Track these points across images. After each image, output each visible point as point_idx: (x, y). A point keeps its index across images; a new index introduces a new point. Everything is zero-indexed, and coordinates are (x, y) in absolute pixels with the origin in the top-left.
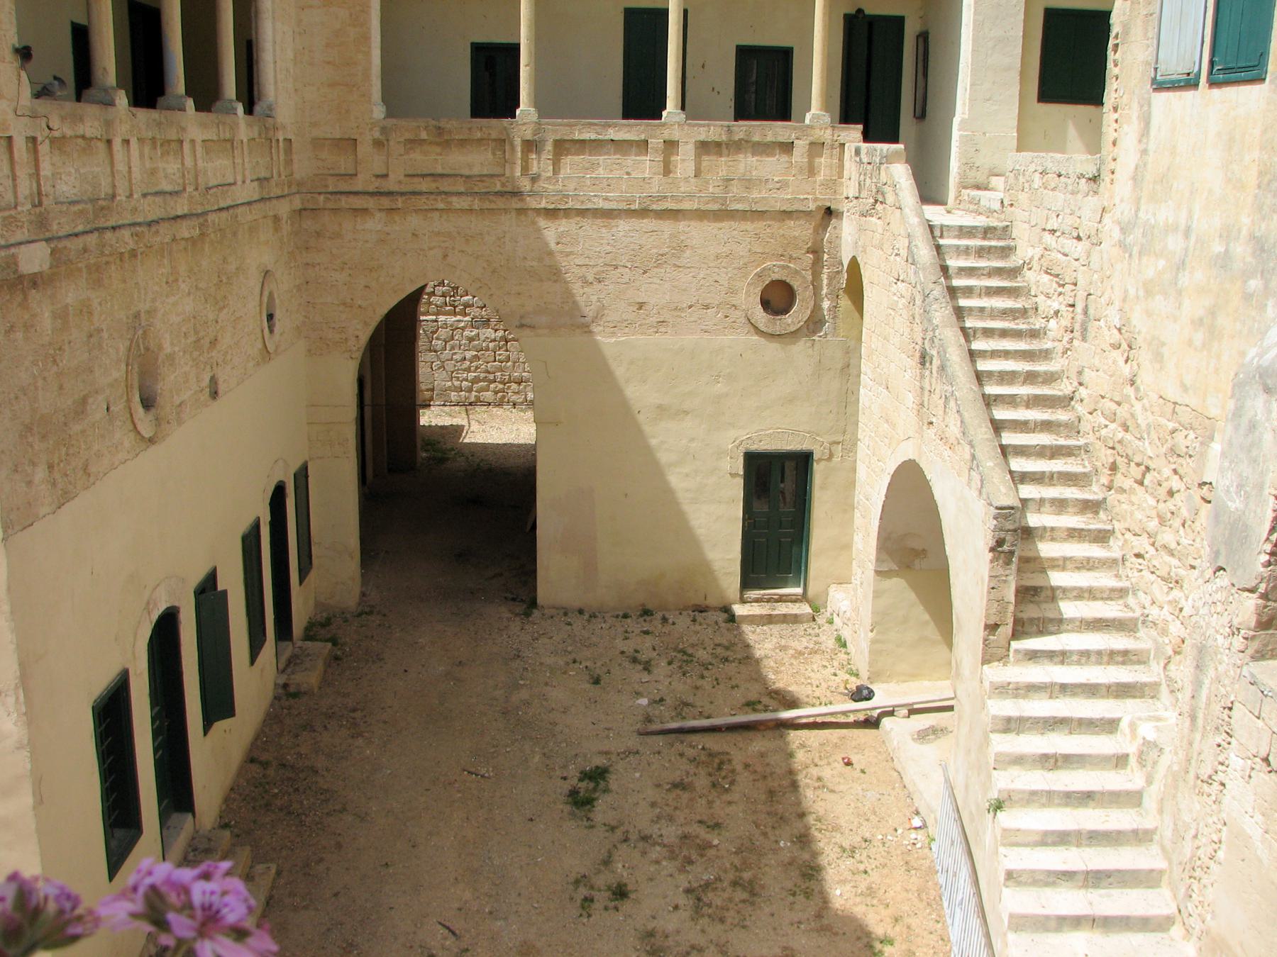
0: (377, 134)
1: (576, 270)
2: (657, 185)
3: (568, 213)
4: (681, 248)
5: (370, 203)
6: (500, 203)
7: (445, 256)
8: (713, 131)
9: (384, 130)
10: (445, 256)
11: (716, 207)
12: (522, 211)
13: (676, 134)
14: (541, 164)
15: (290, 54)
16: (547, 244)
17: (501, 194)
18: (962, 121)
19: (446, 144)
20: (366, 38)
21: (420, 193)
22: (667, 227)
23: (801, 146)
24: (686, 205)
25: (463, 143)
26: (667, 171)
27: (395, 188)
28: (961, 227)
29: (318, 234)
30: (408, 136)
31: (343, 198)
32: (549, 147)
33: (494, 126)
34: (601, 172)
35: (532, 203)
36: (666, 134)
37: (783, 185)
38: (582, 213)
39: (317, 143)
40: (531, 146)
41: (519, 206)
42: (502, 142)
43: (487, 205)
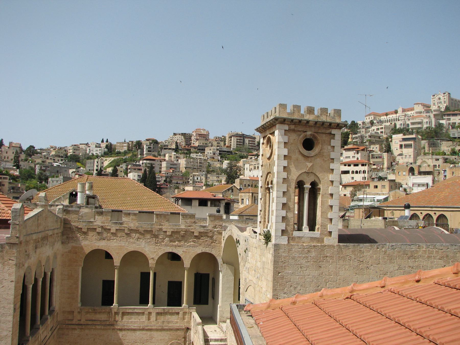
0: (79, 310)
1: (126, 343)
2: (146, 323)
3: (125, 330)
4: (152, 338)
5: (76, 327)
6: (108, 327)
7: (94, 340)
8: (160, 309)
9: (81, 309)
10: (94, 340)
11: (160, 328)
12: (113, 329)
13: (151, 310)
14: (118, 318)
15: (59, 291)
16: (119, 337)
17: (109, 325)
18: (220, 306)
19: (96, 313)
20: (77, 287)
21: (89, 325)
22: (149, 333)
23: (181, 313)
24: (153, 328)
25: (100, 313)
26: (149, 319)
27: (82, 323)
28: (215, 339)
29: (63, 334)
30: (86, 311)
31: (70, 326)
32: (121, 314)
33: (108, 307)
34: (133, 320)
35: (117, 327)
36: (149, 311)
37: (177, 322)
38: (128, 330)
39: (64, 312)
40: (116, 313)
41: (113, 328)
42: (110, 312)
43: (105, 328)
